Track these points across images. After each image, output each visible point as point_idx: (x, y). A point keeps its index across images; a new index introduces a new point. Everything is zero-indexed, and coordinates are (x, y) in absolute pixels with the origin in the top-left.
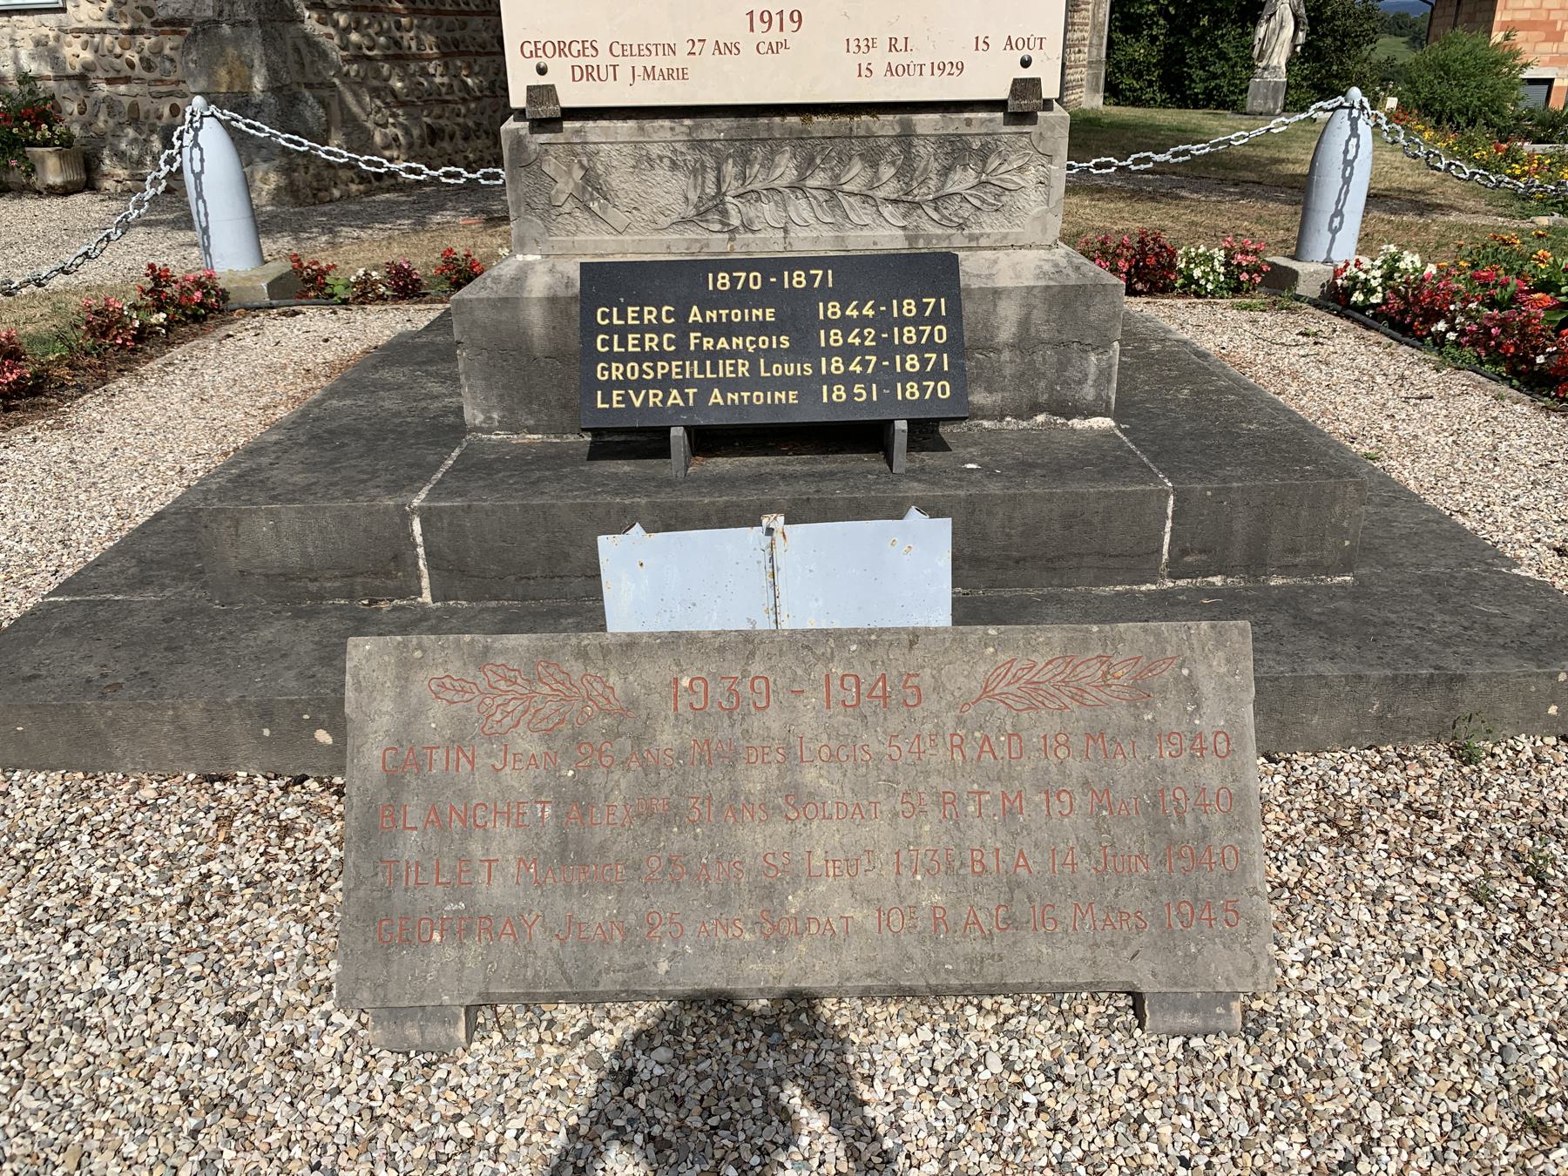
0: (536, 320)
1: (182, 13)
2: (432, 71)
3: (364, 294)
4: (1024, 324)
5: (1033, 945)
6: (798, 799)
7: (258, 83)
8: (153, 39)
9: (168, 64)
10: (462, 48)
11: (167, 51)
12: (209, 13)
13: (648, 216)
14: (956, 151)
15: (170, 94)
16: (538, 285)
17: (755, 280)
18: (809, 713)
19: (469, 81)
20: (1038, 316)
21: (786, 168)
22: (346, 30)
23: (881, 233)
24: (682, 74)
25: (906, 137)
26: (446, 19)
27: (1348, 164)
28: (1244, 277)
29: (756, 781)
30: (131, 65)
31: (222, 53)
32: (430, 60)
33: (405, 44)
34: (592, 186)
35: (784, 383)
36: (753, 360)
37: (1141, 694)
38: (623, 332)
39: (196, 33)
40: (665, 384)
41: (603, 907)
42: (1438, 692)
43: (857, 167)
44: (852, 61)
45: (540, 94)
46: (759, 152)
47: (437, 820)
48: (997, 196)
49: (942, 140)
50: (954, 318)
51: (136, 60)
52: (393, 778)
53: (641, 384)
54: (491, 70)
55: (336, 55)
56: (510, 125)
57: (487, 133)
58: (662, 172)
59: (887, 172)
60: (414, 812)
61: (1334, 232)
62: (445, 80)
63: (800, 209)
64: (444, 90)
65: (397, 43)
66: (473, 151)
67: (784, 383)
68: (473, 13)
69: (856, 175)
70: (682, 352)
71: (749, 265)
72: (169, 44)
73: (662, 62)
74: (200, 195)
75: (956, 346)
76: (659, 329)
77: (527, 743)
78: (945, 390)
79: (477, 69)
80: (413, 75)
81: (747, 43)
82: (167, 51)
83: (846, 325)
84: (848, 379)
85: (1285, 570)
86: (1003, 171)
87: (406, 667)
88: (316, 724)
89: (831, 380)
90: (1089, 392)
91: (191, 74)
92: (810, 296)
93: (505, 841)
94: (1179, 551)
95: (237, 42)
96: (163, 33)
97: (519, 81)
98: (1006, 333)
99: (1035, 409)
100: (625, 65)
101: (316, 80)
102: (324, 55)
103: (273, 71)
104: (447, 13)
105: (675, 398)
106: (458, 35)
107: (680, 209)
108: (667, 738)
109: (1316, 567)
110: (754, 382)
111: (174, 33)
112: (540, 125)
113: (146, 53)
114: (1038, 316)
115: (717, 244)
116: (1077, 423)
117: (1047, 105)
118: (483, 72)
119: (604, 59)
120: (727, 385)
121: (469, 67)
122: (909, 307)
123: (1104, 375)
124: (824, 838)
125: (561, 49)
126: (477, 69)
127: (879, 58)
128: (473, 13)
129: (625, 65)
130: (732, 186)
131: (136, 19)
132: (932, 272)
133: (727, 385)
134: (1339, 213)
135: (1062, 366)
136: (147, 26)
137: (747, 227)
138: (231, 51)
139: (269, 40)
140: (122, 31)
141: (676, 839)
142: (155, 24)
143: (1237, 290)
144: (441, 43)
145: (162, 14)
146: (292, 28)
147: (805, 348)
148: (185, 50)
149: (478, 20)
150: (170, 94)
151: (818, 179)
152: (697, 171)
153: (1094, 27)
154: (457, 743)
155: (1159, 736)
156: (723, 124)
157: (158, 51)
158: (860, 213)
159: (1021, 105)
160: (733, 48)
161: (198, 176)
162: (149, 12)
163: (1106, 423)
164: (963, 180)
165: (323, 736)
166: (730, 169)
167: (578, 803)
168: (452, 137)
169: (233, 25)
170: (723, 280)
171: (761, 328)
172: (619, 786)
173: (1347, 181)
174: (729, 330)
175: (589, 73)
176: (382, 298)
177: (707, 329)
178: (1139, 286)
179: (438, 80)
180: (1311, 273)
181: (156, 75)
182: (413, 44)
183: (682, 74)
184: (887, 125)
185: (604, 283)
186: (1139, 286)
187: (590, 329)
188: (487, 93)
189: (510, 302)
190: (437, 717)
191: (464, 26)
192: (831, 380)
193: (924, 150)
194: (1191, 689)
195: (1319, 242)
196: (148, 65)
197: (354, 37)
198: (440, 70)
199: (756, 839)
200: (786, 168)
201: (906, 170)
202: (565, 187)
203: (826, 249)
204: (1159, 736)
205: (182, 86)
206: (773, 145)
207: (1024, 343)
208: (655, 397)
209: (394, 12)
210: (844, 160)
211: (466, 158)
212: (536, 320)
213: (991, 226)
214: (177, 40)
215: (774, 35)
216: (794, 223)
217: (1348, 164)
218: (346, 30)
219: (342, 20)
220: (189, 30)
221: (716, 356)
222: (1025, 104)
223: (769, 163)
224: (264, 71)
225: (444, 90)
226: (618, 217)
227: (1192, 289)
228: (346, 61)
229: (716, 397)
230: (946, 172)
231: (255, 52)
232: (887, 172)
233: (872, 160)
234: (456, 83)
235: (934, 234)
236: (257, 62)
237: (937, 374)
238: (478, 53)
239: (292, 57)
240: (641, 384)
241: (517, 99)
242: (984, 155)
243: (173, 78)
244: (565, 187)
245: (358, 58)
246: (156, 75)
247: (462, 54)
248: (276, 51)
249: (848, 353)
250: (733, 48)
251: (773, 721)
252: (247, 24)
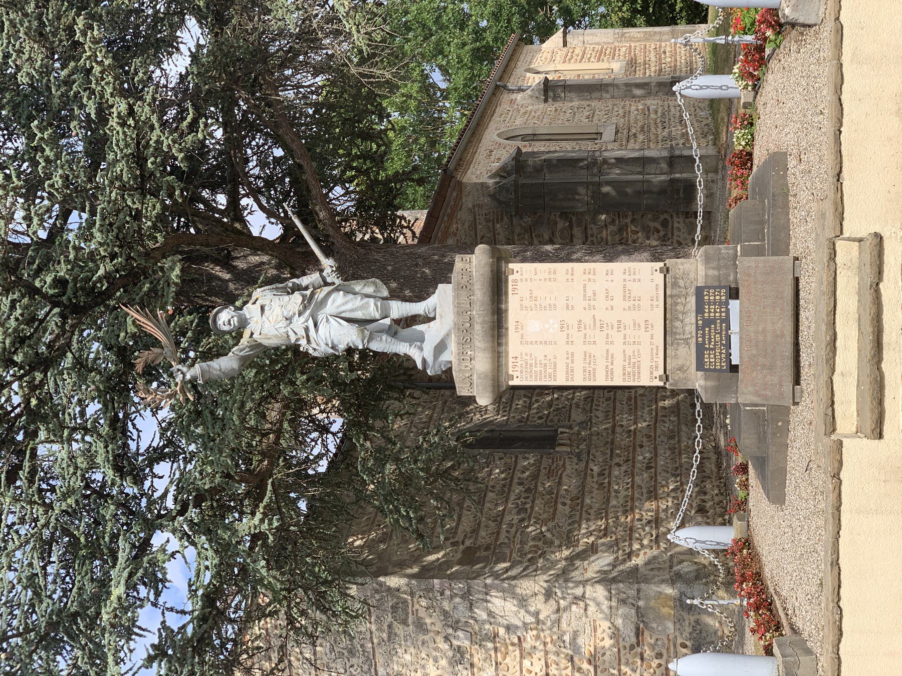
0: (710, 383)
1: (633, 627)
2: (665, 507)
3: (745, 485)
4: (713, 268)
5: (785, 295)
6: (764, 331)
7: (669, 591)
8: (646, 648)
9: (659, 643)
10: (652, 489)
11: (652, 641)
12: (633, 611)
13: (686, 355)
14: (675, 285)
15: (675, 646)
16: (702, 382)
17: (700, 332)
18: (751, 329)
19: (671, 488)
20: (712, 265)
21: (678, 324)
22: (642, 546)
23: (692, 300)
24: (657, 347)
25: (672, 296)
26: (636, 495)
27: (701, 88)
28: (746, 123)
29: (761, 338)
30: (660, 665)
31: (653, 608)
32: (659, 507)
33: (649, 518)
34: (680, 369)
35: (721, 327)
36: (716, 333)
37: (749, 275)
38: (710, 362)
39: (643, 621)
40: (721, 353)
41: (779, 363)
42: (776, 198)
43: (678, 307)
44: (656, 310)
45: (661, 379)
46: (674, 330)
47: (765, 389)
48: (686, 274)
49: (672, 288)
50: (709, 288)
51: (657, 661)
52: (759, 396)
53: (721, 359)
54: (665, 475)
55: (655, 552)
56: (667, 386)
57: (703, 481)
58: (678, 352)
59: (679, 300)
60: (764, 392)
61: (728, 88)
62: (670, 500)
63: (687, 321)
64: (676, 502)
65: (649, 522)
66: (713, 490)
67: (721, 327)
68: (633, 481)
69: (680, 308)
70: (714, 349)
71: (697, 334)
72: (648, 639)
73: (655, 351)
74: (704, 542)
75: (714, 288)
76: (709, 354)
77: (754, 374)
78: (723, 291)
79: (664, 482)
80: (667, 517)
81: (651, 332)
82: (652, 641)
83: (710, 312)
84: (721, 312)
85: (764, 215)
86: (679, 273)
87: (743, 393)
88: (777, 425)
89: (721, 316)
90: (731, 252)
91: (664, 630)
92: (703, 320)
93: (769, 378)
94: (758, 240)
95: (648, 599)
96: (643, 641)
97: (658, 383)
98: (716, 273)
99: (735, 264)
100: (655, 359)
101: (668, 564)
102: (655, 558)
103: (663, 581)
104: (633, 494)
105: (724, 351)
106: (644, 491)
107: (687, 349)
108: (754, 352)
109: (763, 208)
110: (721, 333)
111: (643, 634)
112: (667, 379)
113: (653, 654)
114: (712, 265)
115: (694, 340)
116: (739, 254)
117: (665, 265)
118: (667, 480)
119: (654, 364)
120: (721, 340)
121: (663, 486)
122: (706, 298)
123: (726, 248)
124: (769, 327)
125: (651, 373)
126: (664, 482)
127: (655, 303)
128: (633, 481)
129: (655, 359)
130: (682, 337)
131: (635, 656)
132: (699, 292)
133: (721, 340)
134: (721, 88)
135: (724, 258)
136: (639, 650)
137: (691, 333)
138: (652, 603)
139: (647, 581)
140: (642, 666)
141: (769, 351)
142: (638, 645)
143: (752, 124)
144: (649, 499)
145: (634, 640)
146: (641, 570)
147: (713, 321)
148: (651, 630)
149: (637, 478)
150: (675, 646)
151: (680, 316)
152: (678, 344)
153: (647, 40)
154: (755, 385)
155: (756, 273)
156: (668, 338)
157: (652, 647)
158: (688, 306)
159: (666, 271)
160: (652, 335)
161: (697, 541)
162: (632, 647)
163: (739, 246)
164: (681, 283)
165: (780, 424)
166: (678, 337)
167: (764, 366)
168: (704, 501)
169: (639, 599)
170: (700, 339)
171: (710, 331)
172: (761, 360)
173: (708, 87)
174: (710, 339)
175: (657, 368)
176: (747, 480)
177: (710, 344)
178: (749, 165)
179: (670, 504)
180: (746, 96)
181: (664, 652)
182: (650, 514)
183: (657, 347)
184: (669, 300)
185: (700, 366)
186: (749, 165)
187: (709, 370)
188: (678, 479)
189: (706, 389)
190: (750, 389)
191: (640, 487)
192: (721, 316)
193: (675, 292)
194: (749, 267)
195: (731, 93)
196: (659, 655)
197: (645, 542)
198: (664, 502)
199: (769, 338)
200: (678, 324)
201: (679, 296)
202: (681, 375)
203: (694, 314)
204: (756, 273)
205: (671, 637)
206: (672, 327)
207: (718, 268)
208: (723, 356)
209: (632, 521)
210: (676, 310)
211: (717, 495)
212: (710, 383)
213: (692, 275)
214: (647, 633)
215: (650, 326)
216: (690, 321)
217: (701, 88)
218: (642, 546)
219: (636, 546)
220: (641, 626)
221: (715, 342)
222: (665, 270)
223: (677, 328)
224: (663, 586)
225: (676, 502)
226: (688, 363)
227: (751, 143)
228: (658, 547)
229: (724, 342)
230: (680, 287)
231: (652, 589)
232: (679, 300)
233: (677, 304)
234: (672, 494)
235: (693, 290)
236: (658, 589)
237: (720, 292)
238: (656, 481)
239: (656, 572)
240: (721, 359)
241: (661, 384)
242: (676, 278)
243: (666, 642)
244: (681, 375)
245: (657, 540)
246: (664, 652)
247: (655, 489)
248: (653, 578)
249: (715, 312)
250: (652, 335)
251: (752, 335)
252: (639, 591)
